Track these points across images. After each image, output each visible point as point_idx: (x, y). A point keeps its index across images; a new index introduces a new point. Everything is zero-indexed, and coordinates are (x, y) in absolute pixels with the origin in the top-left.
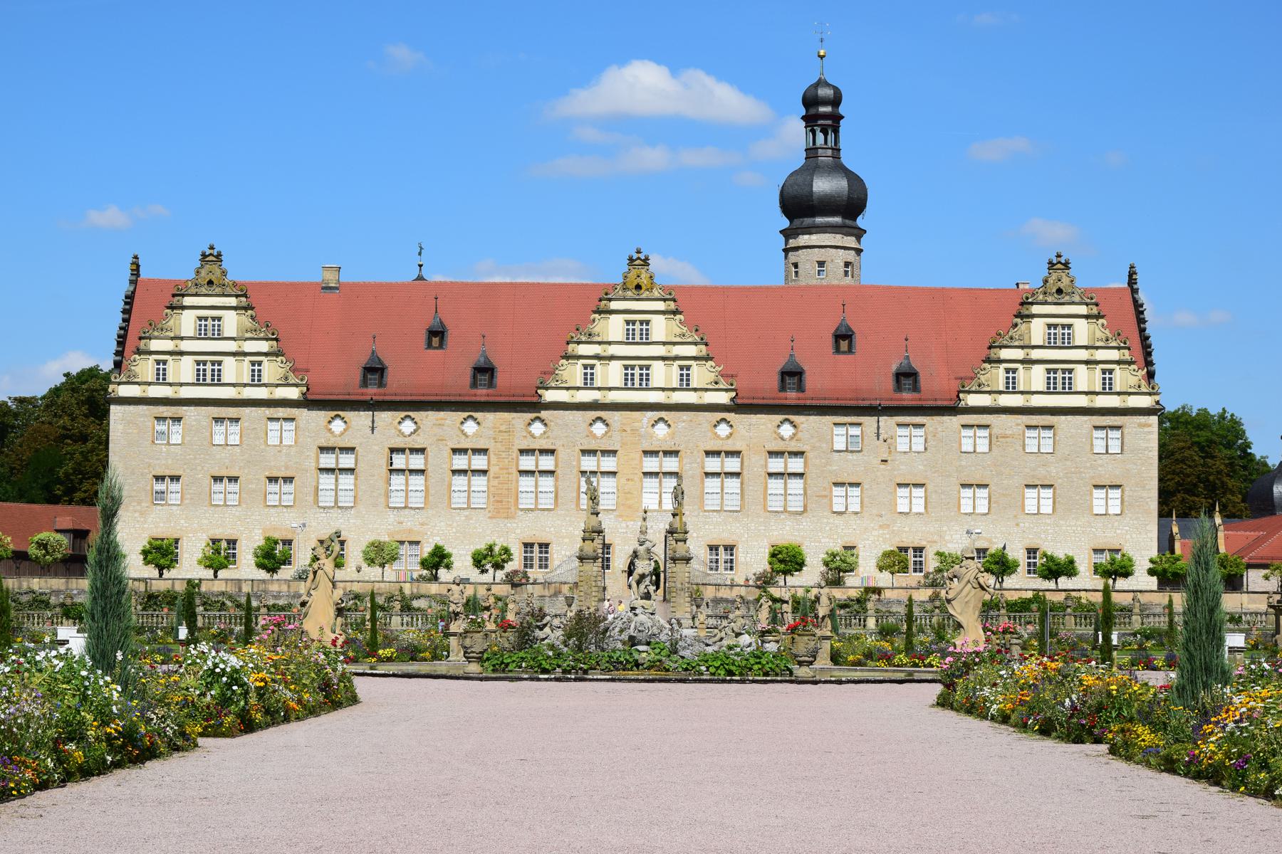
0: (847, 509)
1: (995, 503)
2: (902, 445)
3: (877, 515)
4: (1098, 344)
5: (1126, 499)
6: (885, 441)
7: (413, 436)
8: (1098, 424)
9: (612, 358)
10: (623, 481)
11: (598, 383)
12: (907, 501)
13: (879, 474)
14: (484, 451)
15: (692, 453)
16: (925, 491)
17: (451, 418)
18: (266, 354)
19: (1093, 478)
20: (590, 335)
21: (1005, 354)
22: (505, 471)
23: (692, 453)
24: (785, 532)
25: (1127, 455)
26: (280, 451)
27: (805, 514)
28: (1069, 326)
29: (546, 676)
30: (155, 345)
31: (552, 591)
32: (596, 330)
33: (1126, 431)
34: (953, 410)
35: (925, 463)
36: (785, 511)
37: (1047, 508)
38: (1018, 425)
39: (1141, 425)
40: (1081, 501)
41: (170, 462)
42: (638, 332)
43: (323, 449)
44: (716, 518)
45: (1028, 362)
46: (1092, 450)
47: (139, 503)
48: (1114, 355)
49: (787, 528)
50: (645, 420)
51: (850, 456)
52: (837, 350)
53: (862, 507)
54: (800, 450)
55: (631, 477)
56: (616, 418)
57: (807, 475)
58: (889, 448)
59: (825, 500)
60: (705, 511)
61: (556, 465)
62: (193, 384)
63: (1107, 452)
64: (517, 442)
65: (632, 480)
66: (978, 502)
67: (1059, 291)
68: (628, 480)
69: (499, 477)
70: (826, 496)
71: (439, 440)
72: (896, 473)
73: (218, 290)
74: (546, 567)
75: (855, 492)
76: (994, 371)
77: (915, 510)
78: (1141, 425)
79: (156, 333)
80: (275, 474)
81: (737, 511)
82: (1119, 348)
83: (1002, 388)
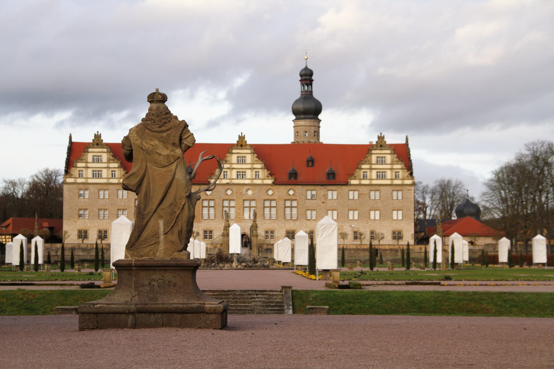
0: (311, 218)
2: (330, 197)
4: (395, 163)
5: (404, 214)
9: (233, 168)
10: (237, 210)
11: (229, 177)
15: (260, 200)
18: (117, 168)
21: (363, 166)
26: (122, 201)
28: (385, 157)
30: (79, 165)
31: (214, 246)
33: (404, 192)
34: (346, 184)
37: (377, 217)
38: (367, 190)
41: (84, 204)
42: (241, 160)
44: (268, 222)
45: (371, 169)
47: (74, 218)
48: (399, 166)
49: (292, 225)
50: (244, 190)
51: (312, 201)
52: (308, 166)
59: (304, 216)
60: (264, 219)
61: (215, 205)
62: (92, 178)
63: (397, 199)
67: (381, 146)
68: (239, 209)
70: (304, 214)
72: (327, 206)
73: (100, 146)
74: (212, 238)
76: (360, 172)
79: (79, 161)
80: (120, 208)
82: (401, 164)
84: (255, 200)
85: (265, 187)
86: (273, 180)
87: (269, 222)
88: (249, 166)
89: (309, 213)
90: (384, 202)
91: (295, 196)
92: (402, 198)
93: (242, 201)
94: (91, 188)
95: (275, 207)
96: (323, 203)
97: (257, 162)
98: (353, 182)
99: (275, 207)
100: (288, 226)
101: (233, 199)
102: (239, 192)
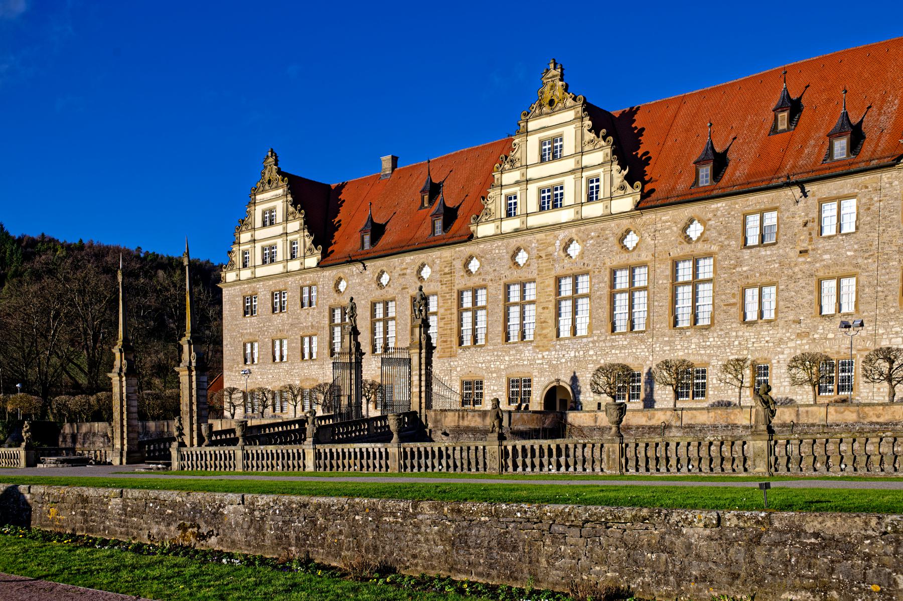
3: (794, 322)
6: (805, 225)
7: (387, 288)
10: (540, 310)
13: (796, 269)
15: (599, 272)
22: (449, 312)
23: (599, 272)
24: (690, 352)
26: (308, 314)
27: (712, 328)
29: (831, 525)
32: (518, 155)
35: (856, 247)
44: (622, 341)
49: (693, 346)
51: (763, 252)
53: (776, 313)
55: (545, 305)
56: (533, 245)
58: (810, 234)
64: (457, 282)
65: (547, 308)
68: (544, 308)
69: (444, 318)
70: (734, 304)
72: (818, 265)
81: (642, 332)
84: (587, 274)
85: (613, 224)
86: (638, 198)
87: (625, 343)
88: (570, 164)
89: (752, 295)
93: (552, 282)
95: (644, 289)
97: (590, 147)
99: (644, 289)
100: (681, 353)
101: (530, 276)
102: (543, 254)
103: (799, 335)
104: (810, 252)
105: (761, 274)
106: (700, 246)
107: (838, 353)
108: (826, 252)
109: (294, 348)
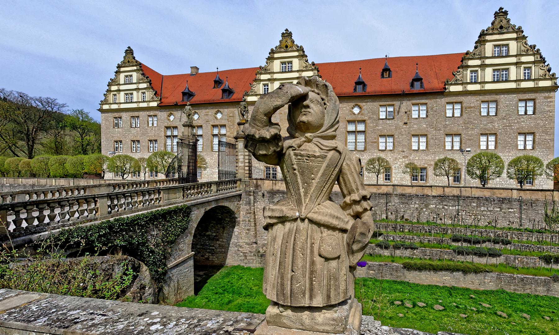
0: (386, 148)
1: (464, 144)
2: (415, 115)
3: (402, 151)
7: (198, 120)
8: (521, 98)
12: (417, 144)
13: (403, 130)
14: (224, 126)
16: (427, 139)
17: (211, 111)
19: (518, 128)
20: (265, 70)
25: (537, 115)
33: (537, 101)
34: (441, 93)
35: (427, 123)
36: (356, 150)
39: (545, 98)
40: (511, 142)
43: (167, 128)
46: (518, 113)
54: (363, 119)
57: (367, 132)
66: (455, 144)
70: (375, 142)
71: (207, 121)
75: (390, 140)
77: (421, 148)
78: (545, 98)
83: (468, 81)
90: (504, 119)
91: (362, 114)
92: (534, 113)
94: (124, 115)
96: (406, 123)
98: (453, 89)
103: (403, 157)
104: (408, 124)
105: (387, 131)
106: (359, 116)
107: (420, 165)
108: (415, 124)
109: (144, 146)
